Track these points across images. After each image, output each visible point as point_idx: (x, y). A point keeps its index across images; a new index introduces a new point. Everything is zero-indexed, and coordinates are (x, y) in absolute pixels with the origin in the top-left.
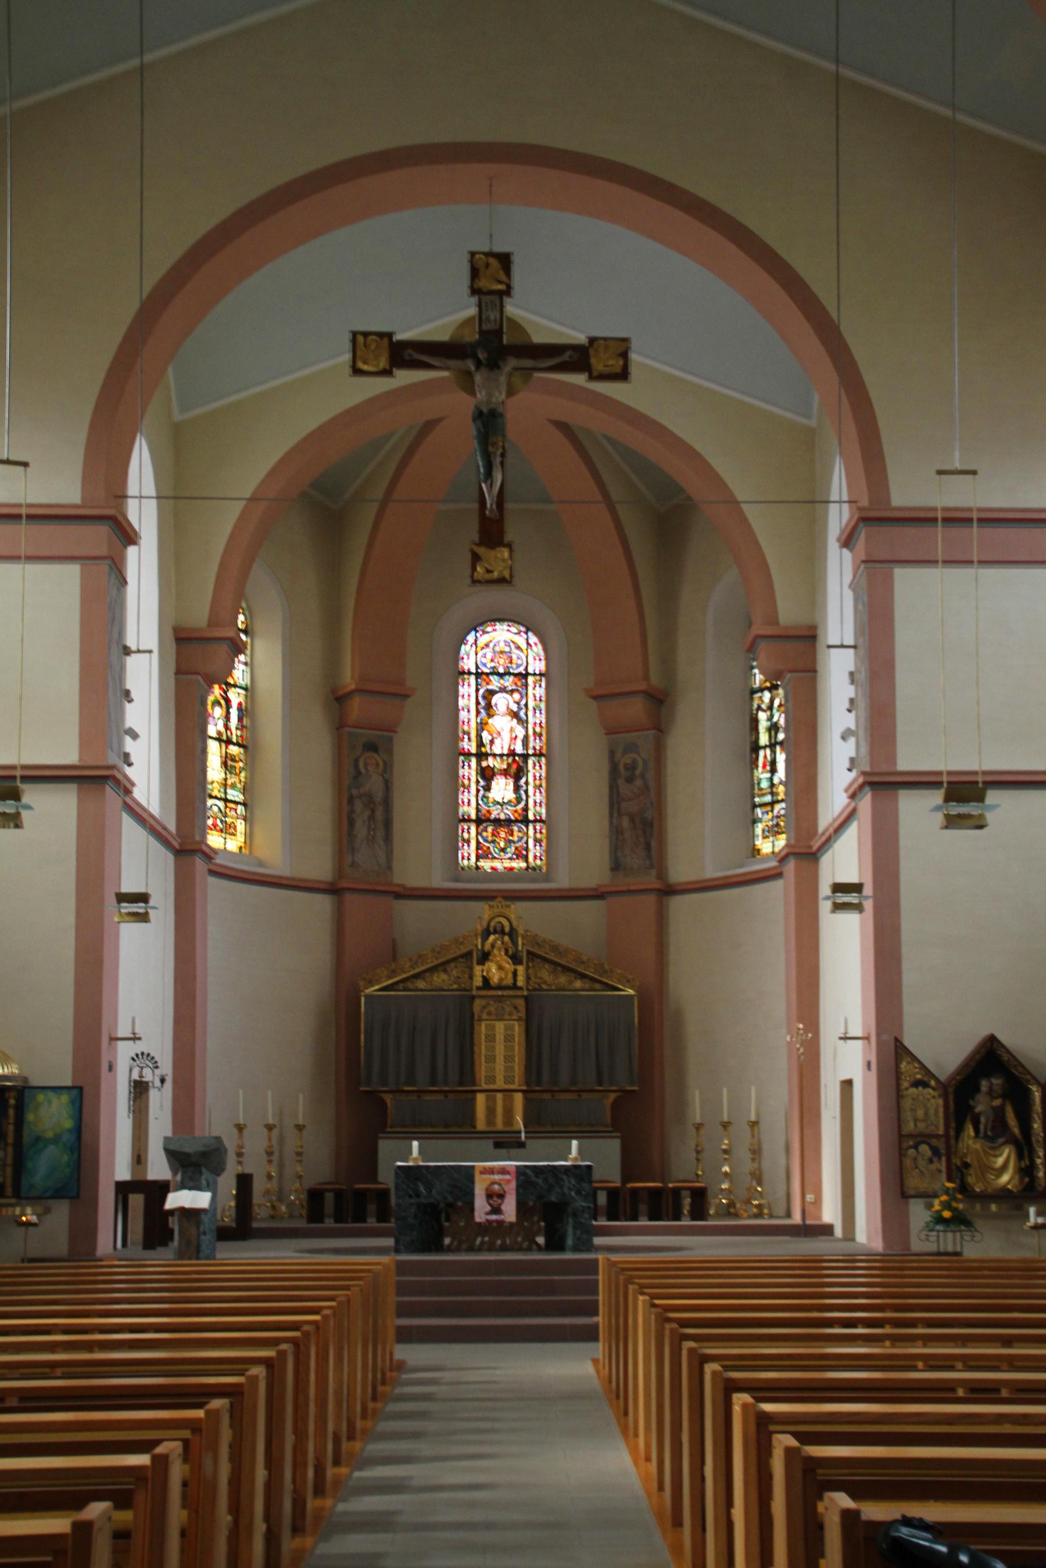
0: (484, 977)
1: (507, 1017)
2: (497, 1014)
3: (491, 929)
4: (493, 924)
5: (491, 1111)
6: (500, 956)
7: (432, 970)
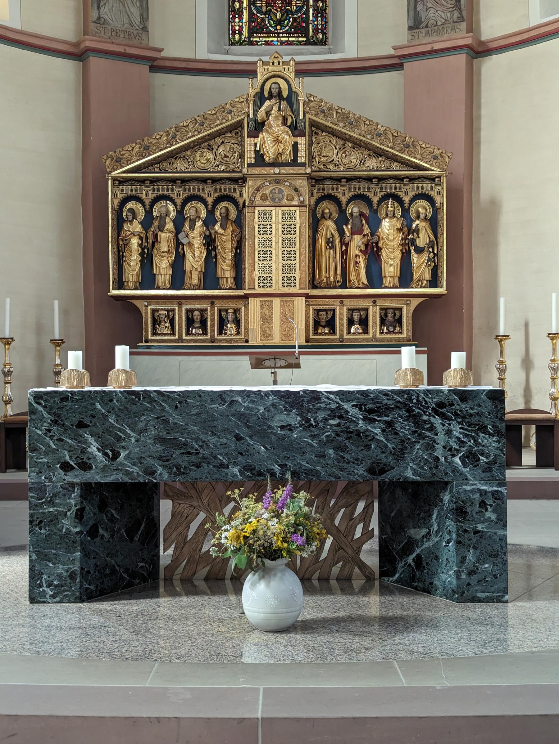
0: (257, 152)
1: (285, 202)
2: (273, 199)
3: (266, 94)
5: (266, 319)
6: (276, 126)
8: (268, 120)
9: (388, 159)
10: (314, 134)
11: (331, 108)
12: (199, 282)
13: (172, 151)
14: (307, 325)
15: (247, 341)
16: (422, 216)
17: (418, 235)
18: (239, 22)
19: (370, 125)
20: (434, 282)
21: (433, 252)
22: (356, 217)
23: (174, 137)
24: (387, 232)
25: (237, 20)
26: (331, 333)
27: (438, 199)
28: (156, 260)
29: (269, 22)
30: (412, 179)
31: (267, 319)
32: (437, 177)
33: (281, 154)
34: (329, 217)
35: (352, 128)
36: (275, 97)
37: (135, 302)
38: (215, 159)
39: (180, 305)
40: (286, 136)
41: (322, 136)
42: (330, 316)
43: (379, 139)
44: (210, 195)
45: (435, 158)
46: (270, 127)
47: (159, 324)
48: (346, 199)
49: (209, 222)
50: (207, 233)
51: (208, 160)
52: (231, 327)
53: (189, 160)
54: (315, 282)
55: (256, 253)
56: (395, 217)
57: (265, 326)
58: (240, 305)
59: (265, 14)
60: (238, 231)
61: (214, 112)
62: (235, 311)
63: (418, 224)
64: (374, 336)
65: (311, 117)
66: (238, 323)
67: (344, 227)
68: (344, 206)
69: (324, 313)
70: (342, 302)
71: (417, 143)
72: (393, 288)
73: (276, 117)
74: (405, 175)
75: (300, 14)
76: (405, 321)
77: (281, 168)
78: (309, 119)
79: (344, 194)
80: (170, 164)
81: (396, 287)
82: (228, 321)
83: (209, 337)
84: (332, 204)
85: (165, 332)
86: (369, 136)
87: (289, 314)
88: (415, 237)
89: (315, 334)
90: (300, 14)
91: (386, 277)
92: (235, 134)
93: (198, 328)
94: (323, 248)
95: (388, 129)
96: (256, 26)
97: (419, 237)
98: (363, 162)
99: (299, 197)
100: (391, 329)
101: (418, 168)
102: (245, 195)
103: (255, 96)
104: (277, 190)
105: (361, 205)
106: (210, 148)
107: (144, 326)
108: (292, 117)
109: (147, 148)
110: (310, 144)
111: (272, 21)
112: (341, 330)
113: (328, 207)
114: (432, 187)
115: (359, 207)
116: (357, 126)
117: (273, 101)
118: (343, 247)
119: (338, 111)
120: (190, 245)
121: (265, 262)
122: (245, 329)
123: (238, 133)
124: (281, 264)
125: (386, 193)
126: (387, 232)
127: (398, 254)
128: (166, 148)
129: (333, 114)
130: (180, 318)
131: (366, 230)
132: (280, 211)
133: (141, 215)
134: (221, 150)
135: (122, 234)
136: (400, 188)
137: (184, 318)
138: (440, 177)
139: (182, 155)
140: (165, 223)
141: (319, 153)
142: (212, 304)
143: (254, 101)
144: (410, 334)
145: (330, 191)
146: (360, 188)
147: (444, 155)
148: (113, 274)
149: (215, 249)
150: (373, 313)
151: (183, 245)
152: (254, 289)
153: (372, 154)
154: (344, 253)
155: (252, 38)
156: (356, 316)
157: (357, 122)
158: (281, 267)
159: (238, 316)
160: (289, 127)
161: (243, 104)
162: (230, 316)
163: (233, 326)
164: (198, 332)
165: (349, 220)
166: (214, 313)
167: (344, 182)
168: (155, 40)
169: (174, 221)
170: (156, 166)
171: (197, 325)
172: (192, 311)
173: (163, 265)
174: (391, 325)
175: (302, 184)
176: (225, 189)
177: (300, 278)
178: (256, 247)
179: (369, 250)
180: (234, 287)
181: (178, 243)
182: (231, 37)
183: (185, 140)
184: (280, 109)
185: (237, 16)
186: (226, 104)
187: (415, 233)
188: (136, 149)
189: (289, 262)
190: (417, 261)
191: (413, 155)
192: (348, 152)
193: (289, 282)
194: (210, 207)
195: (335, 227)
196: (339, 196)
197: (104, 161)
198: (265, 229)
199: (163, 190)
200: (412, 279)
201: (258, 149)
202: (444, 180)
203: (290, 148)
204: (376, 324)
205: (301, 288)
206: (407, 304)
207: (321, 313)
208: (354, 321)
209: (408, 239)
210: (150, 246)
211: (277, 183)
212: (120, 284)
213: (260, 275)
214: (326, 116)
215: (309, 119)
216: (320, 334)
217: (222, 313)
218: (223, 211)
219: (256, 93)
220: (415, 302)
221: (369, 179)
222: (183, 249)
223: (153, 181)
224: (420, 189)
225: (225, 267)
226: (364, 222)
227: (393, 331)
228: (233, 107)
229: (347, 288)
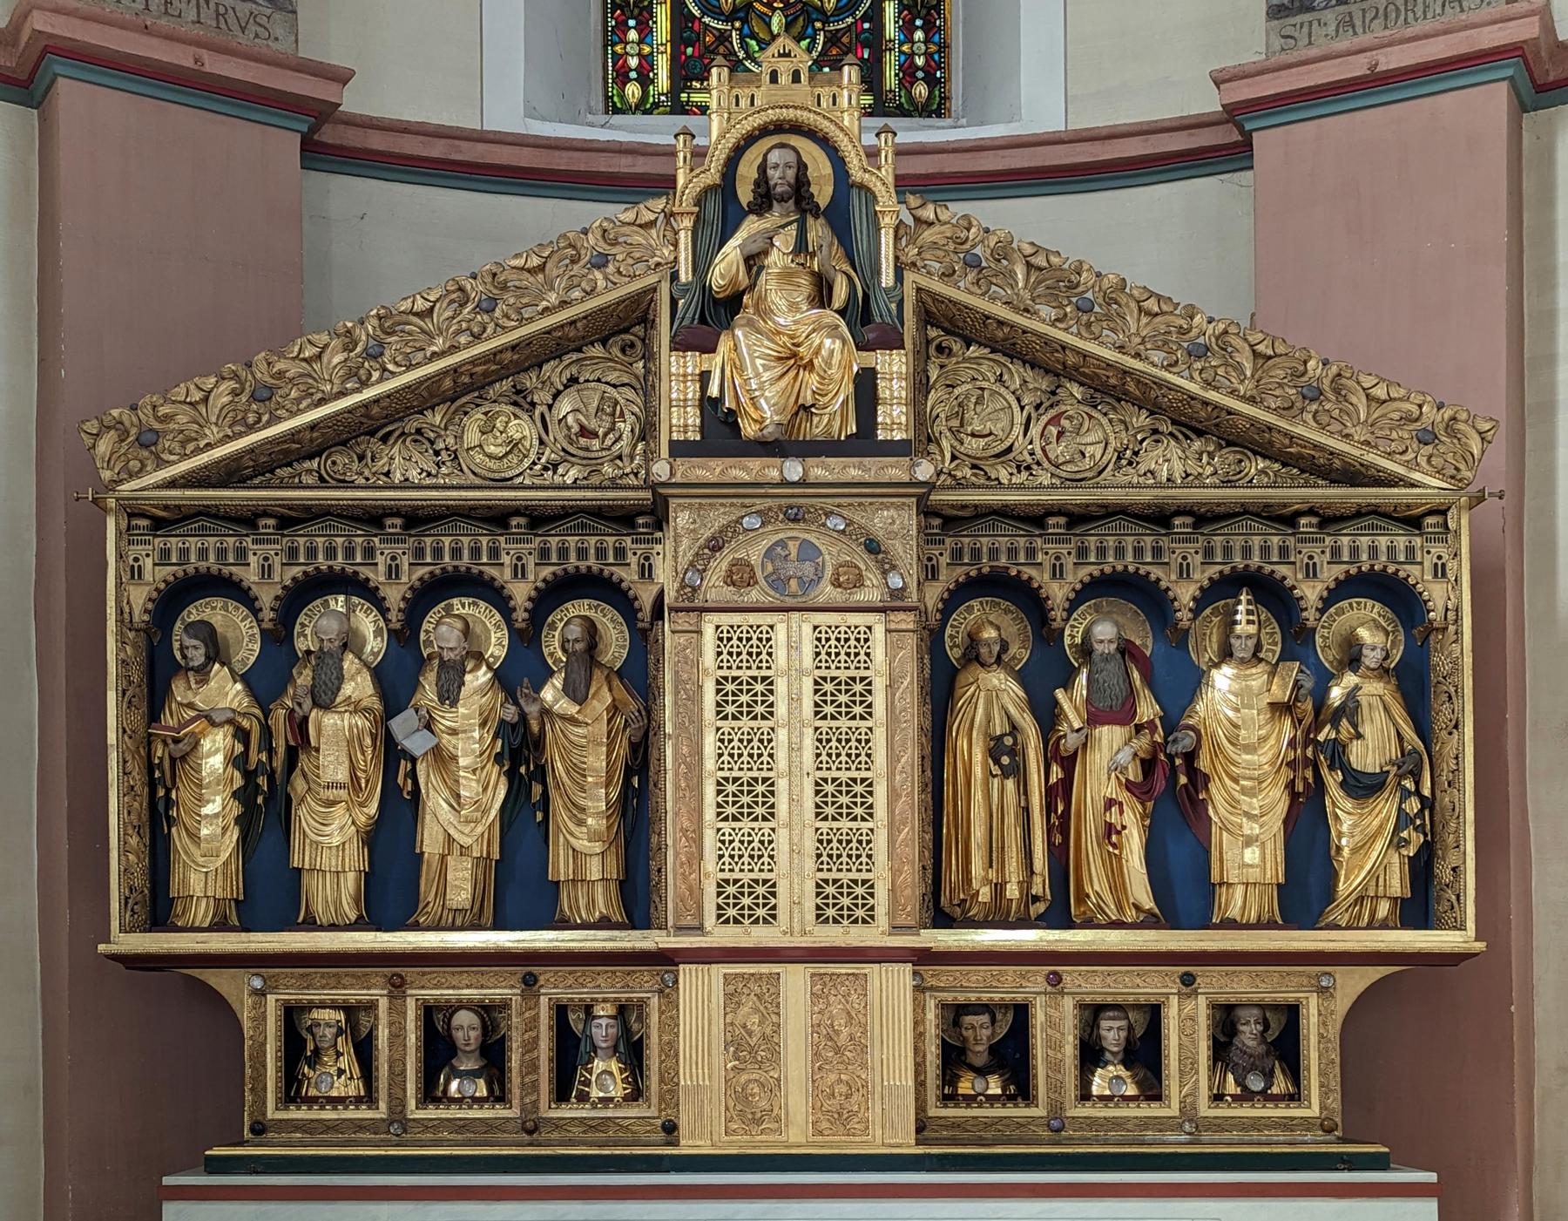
0: (709, 405)
1: (827, 592)
3: (745, 194)
4: (747, 170)
5: (752, 1050)
6: (784, 305)
7: (463, 389)
8: (752, 287)
9: (1229, 444)
10: (932, 351)
11: (1003, 252)
12: (479, 898)
13: (366, 405)
14: (919, 1068)
15: (670, 1128)
16: (1371, 658)
17: (1355, 726)
18: (641, 42)
19: (1163, 313)
20: (1419, 906)
21: (1418, 793)
22: (1107, 658)
23: (375, 354)
24: (1231, 714)
25: (633, 35)
26: (1011, 1098)
27: (1436, 595)
28: (305, 817)
29: (744, 46)
30: (1329, 520)
31: (753, 1051)
32: (1431, 513)
33: (805, 408)
34: (999, 660)
35: (1089, 325)
36: (782, 199)
37: (219, 980)
38: (541, 442)
39: (397, 988)
40: (828, 342)
41: (965, 360)
42: (1002, 1030)
43: (1198, 365)
44: (519, 572)
45: (1427, 438)
46: (764, 312)
47: (315, 1059)
48: (1067, 589)
49: (521, 674)
50: (511, 713)
51: (514, 445)
52: (605, 1075)
53: (440, 445)
54: (944, 901)
55: (710, 790)
56: (1261, 660)
57: (744, 1078)
58: (641, 985)
59: (729, 19)
60: (633, 706)
61: (535, 261)
62: (622, 1011)
63: (1357, 688)
64: (1188, 1111)
65: (924, 282)
66: (632, 1053)
67: (1060, 694)
68: (1058, 614)
69: (985, 1018)
70: (1055, 980)
71: (1350, 383)
72: (1258, 925)
73: (786, 276)
74: (1304, 500)
75: (850, 20)
76: (1314, 1055)
77: (810, 461)
78: (919, 290)
79: (1057, 572)
80: (361, 458)
81: (1271, 925)
82: (595, 1048)
83: (513, 1113)
84: (1007, 611)
85: (334, 1093)
86: (1157, 357)
87: (845, 1032)
88: (1344, 735)
89: (949, 1098)
90: (850, 20)
91: (1229, 885)
92: (623, 351)
93: (472, 1075)
94: (978, 771)
95: (1233, 329)
96: (701, 57)
97: (1359, 736)
98: (1127, 457)
99: (885, 573)
100: (1256, 1084)
101: (1354, 475)
102: (664, 575)
103: (699, 201)
104: (793, 547)
105: (1124, 614)
106: (522, 400)
107: (248, 1071)
108: (849, 278)
109: (264, 395)
110: (920, 386)
111: (753, 43)
112: (1056, 1087)
113: (992, 622)
114: (1410, 550)
115: (1117, 624)
116: (1109, 317)
117: (773, 218)
118: (1055, 768)
119: (1033, 260)
120: (442, 759)
121: (746, 825)
122: (662, 1081)
123: (632, 345)
124: (809, 833)
125: (1227, 569)
126: (1231, 714)
127: (1275, 800)
128: (343, 394)
129: (1013, 274)
130: (399, 1037)
131: (1147, 709)
132: (807, 629)
133: (248, 650)
134: (565, 406)
135: (168, 719)
136: (1284, 551)
137: (412, 1039)
138: (1444, 513)
139: (411, 425)
140: (341, 679)
141: (955, 423)
142: (530, 982)
143: (699, 221)
144: (1335, 1102)
145: (1003, 561)
146: (1123, 550)
147: (1461, 426)
148: (125, 871)
149: (541, 774)
150: (1181, 1021)
151: (414, 760)
152: (699, 929)
153: (1166, 427)
154: (1060, 793)
155: (684, 96)
156: (1112, 1033)
157: (1110, 301)
158: (810, 845)
159: (635, 1027)
160: (842, 312)
161: (653, 232)
162: (603, 1029)
163: (614, 1066)
164: (469, 1090)
165: (1074, 672)
166: (536, 1018)
167: (1057, 525)
168: (324, 34)
169: (378, 674)
170: (307, 465)
171: (466, 1065)
172: (452, 1008)
173: (331, 839)
174: (1253, 1068)
175: (897, 524)
176: (582, 550)
177: (893, 890)
178: (710, 764)
179: (1160, 784)
180: (617, 917)
181: (392, 754)
182: (613, 91)
183: (419, 365)
184: (801, 246)
185: (632, 23)
186: (585, 232)
187: (1344, 722)
188: (221, 397)
189: (845, 824)
190: (1355, 826)
191: (1335, 427)
192: (1070, 418)
193: (846, 901)
194: (521, 615)
195: (1021, 693)
196: (1040, 577)
197: (89, 441)
198: (744, 698)
199: (331, 552)
200: (1329, 894)
201: (714, 391)
202: (1461, 521)
203: (848, 389)
204: (1195, 1062)
205: (896, 929)
206: (1322, 991)
207: (968, 1019)
208: (1103, 1050)
209: (1316, 742)
210: (279, 762)
211: (795, 520)
212: (158, 908)
213: (727, 875)
214: (983, 281)
215: (919, 290)
216: (970, 1100)
217: (572, 1017)
218: (575, 631)
219: (708, 190)
220: (1352, 983)
221: (1159, 518)
222: (413, 775)
223: (291, 519)
224: (1364, 557)
225: (582, 844)
226: (1136, 675)
227: (1263, 1092)
228: (615, 243)
229: (1068, 924)
